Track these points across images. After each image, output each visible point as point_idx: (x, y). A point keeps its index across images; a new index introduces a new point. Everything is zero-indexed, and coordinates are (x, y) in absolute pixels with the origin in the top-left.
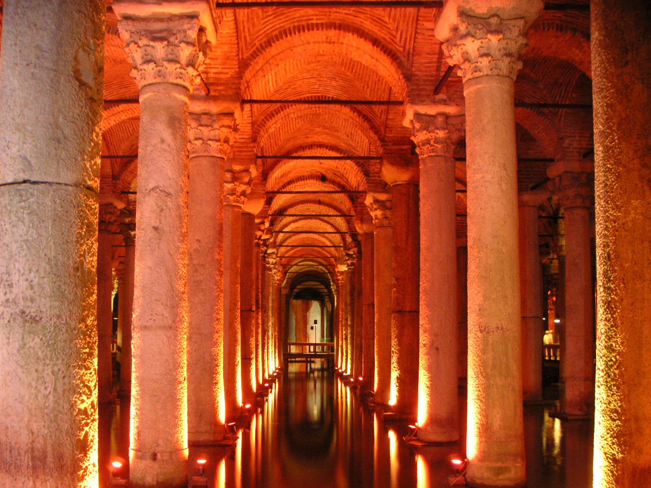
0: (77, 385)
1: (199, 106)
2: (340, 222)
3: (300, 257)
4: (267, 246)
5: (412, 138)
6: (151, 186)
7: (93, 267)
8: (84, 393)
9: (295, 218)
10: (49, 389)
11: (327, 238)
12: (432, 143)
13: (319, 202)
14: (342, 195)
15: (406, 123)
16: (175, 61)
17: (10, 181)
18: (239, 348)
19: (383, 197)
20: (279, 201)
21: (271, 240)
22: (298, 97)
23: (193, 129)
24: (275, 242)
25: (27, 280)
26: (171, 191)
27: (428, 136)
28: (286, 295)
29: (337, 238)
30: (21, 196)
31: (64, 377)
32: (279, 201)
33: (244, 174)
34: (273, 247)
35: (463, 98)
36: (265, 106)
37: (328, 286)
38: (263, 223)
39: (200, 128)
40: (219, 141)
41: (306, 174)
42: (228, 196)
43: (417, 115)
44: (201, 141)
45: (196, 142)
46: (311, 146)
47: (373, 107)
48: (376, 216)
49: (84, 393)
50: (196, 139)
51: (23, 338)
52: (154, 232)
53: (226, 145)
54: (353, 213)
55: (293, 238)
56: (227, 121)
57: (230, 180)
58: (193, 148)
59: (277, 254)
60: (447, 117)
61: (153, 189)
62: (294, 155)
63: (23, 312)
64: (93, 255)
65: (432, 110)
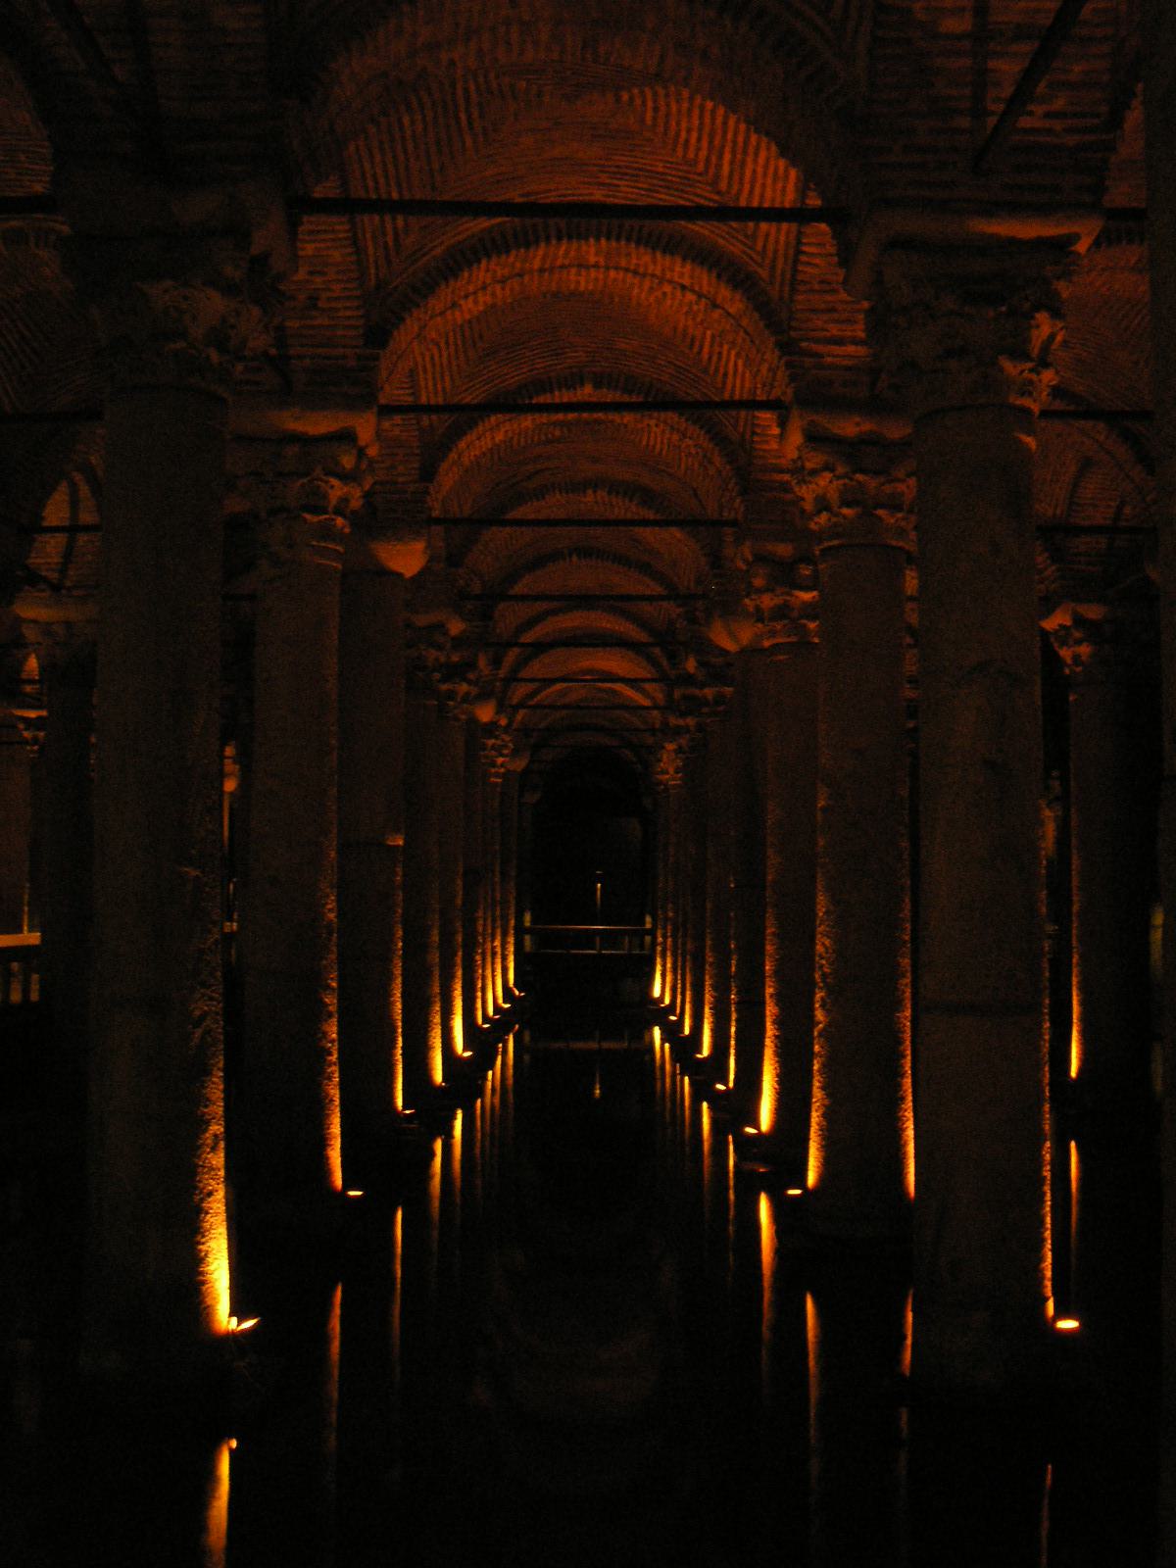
1: (858, 424)
16: (1019, 353)
19: (1094, 612)
23: (838, 478)
39: (859, 477)
40: (898, 508)
42: (804, 621)
44: (859, 510)
45: (845, 511)
48: (1076, 658)
50: (848, 505)
58: (836, 525)
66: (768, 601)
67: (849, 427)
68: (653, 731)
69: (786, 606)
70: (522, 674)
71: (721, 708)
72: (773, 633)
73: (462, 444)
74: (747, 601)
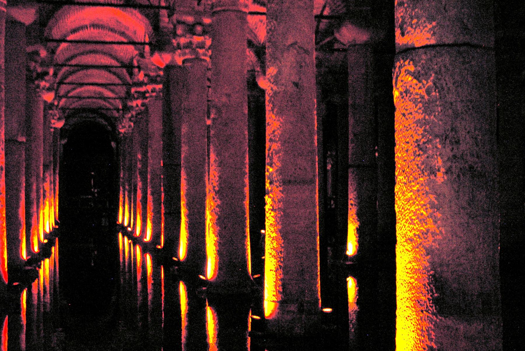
52: (295, 88)
57: (201, 33)
61: (292, 45)
63: (471, 167)
66: (183, 41)
68: (118, 110)
69: (191, 43)
70: (65, 81)
71: (154, 94)
72: (185, 54)
74: (174, 41)
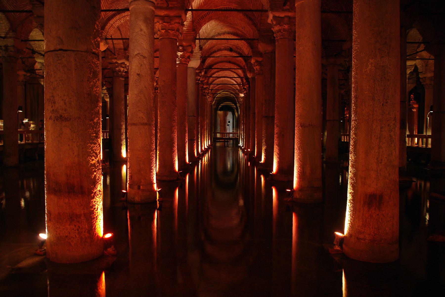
0: (90, 152)
2: (240, 72)
3: (222, 90)
4: (203, 84)
5: (272, 29)
6: (136, 53)
7: (97, 93)
8: (93, 156)
9: (218, 70)
10: (75, 154)
11: (234, 80)
12: (282, 31)
13: (230, 62)
14: (241, 58)
15: (269, 21)
17: (52, 49)
18: (187, 135)
19: (260, 59)
20: (209, 61)
21: (205, 81)
22: (216, 8)
24: (208, 82)
25: (63, 100)
26: (146, 55)
27: (280, 28)
28: (215, 109)
29: (239, 80)
30: (58, 57)
31: (83, 148)
32: (209, 61)
33: (189, 47)
34: (207, 85)
35: (295, 8)
36: (200, 12)
37: (236, 104)
38: (201, 72)
39: (164, 24)
41: (222, 48)
43: (274, 17)
46: (224, 34)
47: (254, 13)
49: (93, 156)
50: (162, 29)
51: (61, 129)
52: (138, 76)
53: (177, 32)
54: (246, 68)
55: (217, 80)
56: (177, 20)
59: (209, 88)
60: (289, 18)
62: (216, 38)
64: (97, 87)
65: (282, 15)
67: (162, 13)
73: (111, 22)
